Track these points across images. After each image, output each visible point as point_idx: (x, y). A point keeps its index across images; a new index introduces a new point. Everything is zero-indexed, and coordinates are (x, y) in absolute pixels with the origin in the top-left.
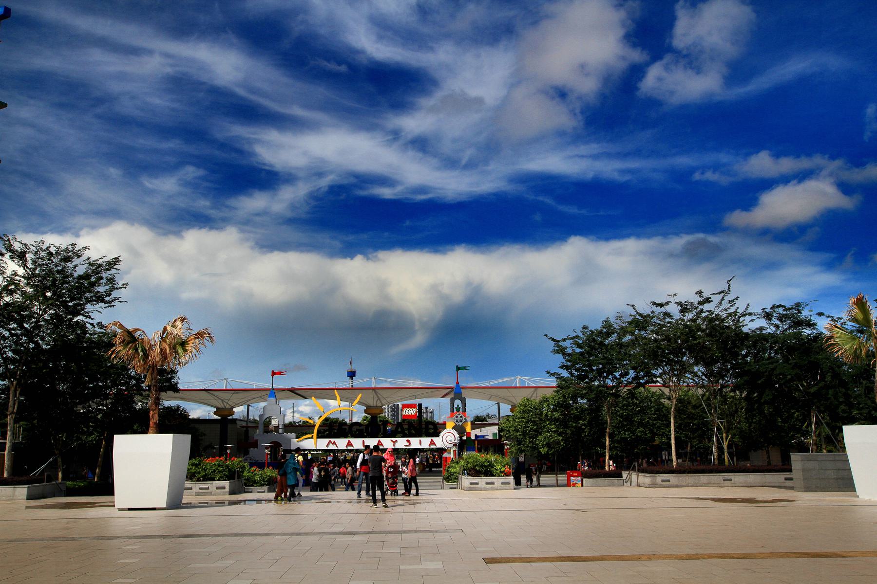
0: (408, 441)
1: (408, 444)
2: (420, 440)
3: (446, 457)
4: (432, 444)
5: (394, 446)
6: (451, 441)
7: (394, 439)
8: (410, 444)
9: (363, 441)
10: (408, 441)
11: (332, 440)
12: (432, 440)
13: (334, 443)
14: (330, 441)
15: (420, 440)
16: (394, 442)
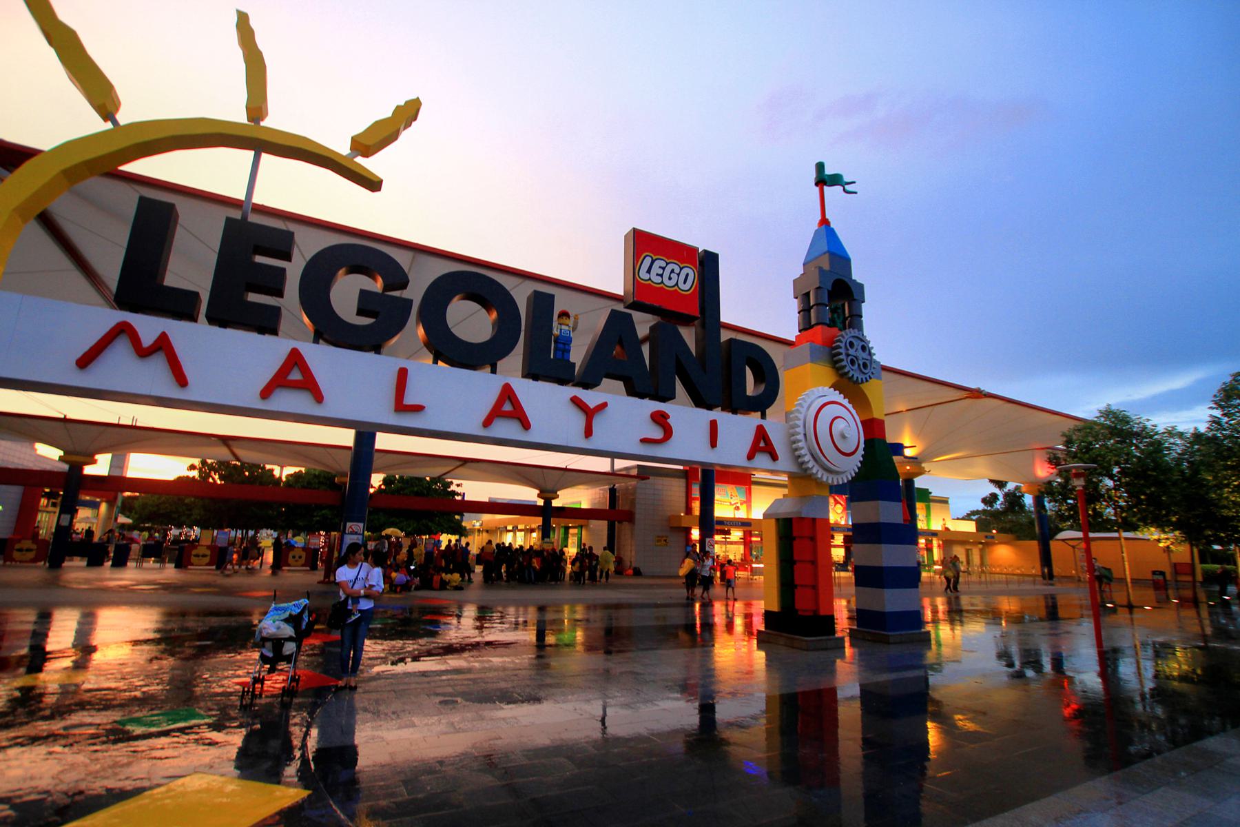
0: (660, 419)
1: (657, 433)
2: (713, 424)
3: (814, 519)
4: (762, 450)
5: (588, 432)
6: (843, 437)
7: (591, 398)
8: (668, 432)
9: (403, 374)
10: (660, 419)
11: (148, 327)
12: (761, 434)
13: (163, 345)
14: (123, 329)
15: (713, 424)
16: (590, 413)
